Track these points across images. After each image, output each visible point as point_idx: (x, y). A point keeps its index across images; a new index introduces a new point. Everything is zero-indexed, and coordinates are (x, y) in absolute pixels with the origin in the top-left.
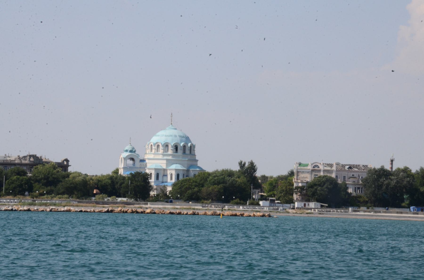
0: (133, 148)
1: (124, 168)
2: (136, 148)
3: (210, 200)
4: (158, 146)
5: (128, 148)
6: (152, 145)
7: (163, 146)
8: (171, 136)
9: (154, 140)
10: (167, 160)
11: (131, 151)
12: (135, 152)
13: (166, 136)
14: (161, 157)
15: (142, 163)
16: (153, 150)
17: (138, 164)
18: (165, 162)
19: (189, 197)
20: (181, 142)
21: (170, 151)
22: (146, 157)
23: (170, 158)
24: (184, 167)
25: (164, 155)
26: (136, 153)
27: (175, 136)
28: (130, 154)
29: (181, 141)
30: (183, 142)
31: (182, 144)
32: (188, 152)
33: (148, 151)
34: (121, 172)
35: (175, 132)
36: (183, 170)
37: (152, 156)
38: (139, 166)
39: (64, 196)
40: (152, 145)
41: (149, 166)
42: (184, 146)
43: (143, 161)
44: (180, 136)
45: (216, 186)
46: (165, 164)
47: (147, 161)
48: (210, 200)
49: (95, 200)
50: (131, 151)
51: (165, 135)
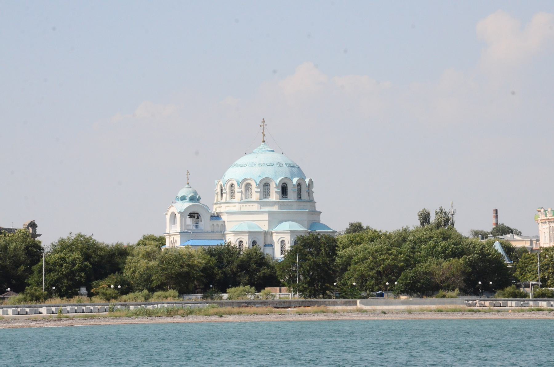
0: (196, 193)
1: (181, 233)
2: (200, 194)
3: (457, 291)
4: (248, 186)
5: (185, 191)
6: (232, 185)
7: (258, 186)
8: (272, 165)
9: (234, 174)
10: (270, 213)
11: (192, 199)
12: (199, 199)
13: (261, 165)
14: (256, 207)
15: (215, 222)
16: (238, 196)
17: (205, 223)
18: (266, 217)
19: (407, 285)
20: (293, 178)
21: (274, 196)
22: (216, 209)
23: (275, 208)
24: (303, 226)
25: (262, 204)
26: (201, 201)
27: (280, 165)
28: (191, 204)
29: (293, 175)
30: (296, 176)
31: (295, 181)
32: (305, 196)
33: (226, 196)
34: (174, 242)
35: (276, 157)
36: (305, 232)
37: (236, 208)
38: (209, 229)
39: (168, 293)
40: (232, 185)
41: (229, 227)
42: (299, 185)
43: (216, 217)
44: (289, 166)
45: (453, 261)
46: (267, 223)
47: (224, 218)
48: (457, 291)
49: (230, 298)
50: (192, 199)
51: (255, 165)
